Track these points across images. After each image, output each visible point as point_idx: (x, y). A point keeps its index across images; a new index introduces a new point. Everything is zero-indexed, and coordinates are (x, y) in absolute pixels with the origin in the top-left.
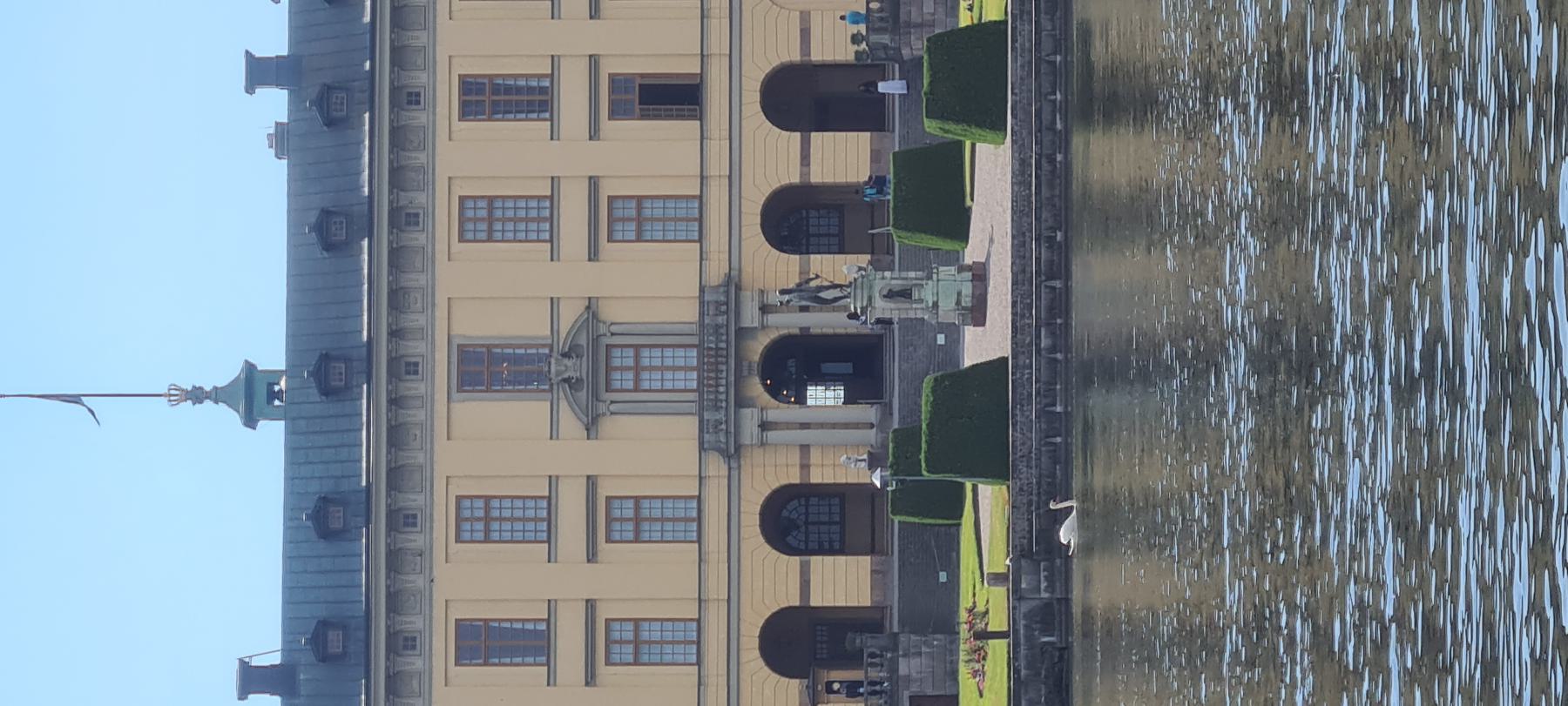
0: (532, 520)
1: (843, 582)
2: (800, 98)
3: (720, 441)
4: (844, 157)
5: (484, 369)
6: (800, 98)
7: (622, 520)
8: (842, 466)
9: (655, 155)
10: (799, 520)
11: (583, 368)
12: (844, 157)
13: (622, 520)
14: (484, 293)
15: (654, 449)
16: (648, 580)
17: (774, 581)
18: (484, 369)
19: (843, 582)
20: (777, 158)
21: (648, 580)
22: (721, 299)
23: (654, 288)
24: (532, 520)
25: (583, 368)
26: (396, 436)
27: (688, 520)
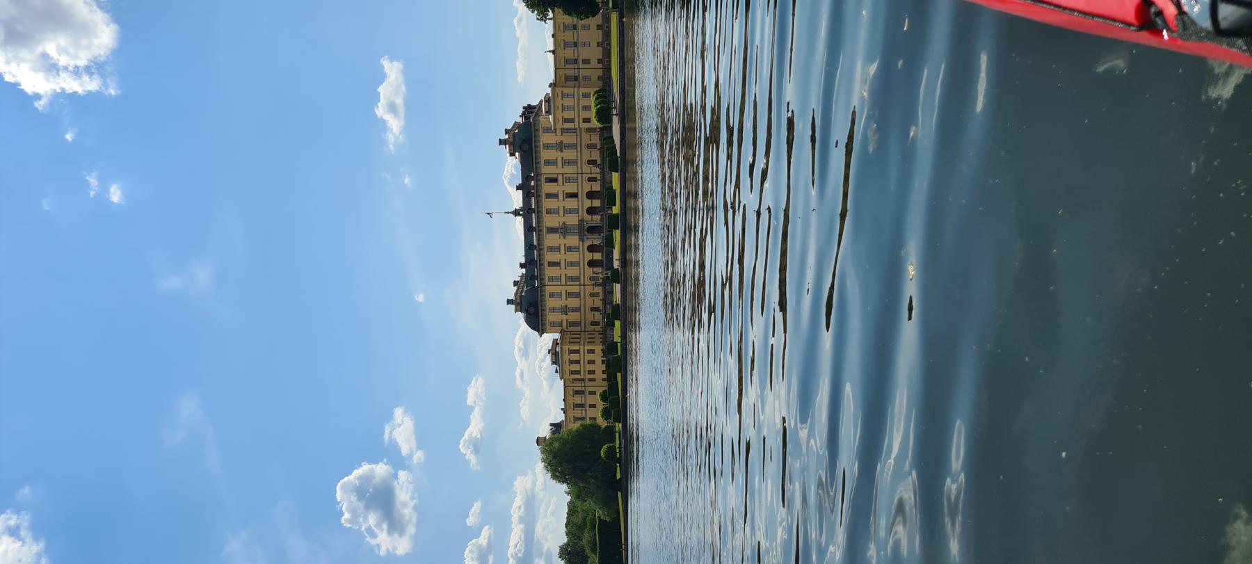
0: (558, 249)
1: (598, 256)
2: (591, 195)
3: (582, 240)
4: (597, 203)
5: (551, 230)
6: (591, 195)
7: (569, 249)
8: (596, 242)
9: (571, 203)
10: (592, 249)
11: (564, 230)
12: (597, 203)
13: (569, 249)
14: (550, 221)
15: (573, 240)
16: (573, 257)
17: (589, 256)
18: (551, 230)
19: (598, 256)
20: (588, 203)
21: (573, 257)
22: (582, 221)
23: (573, 220)
24: (558, 249)
25: (564, 230)
26: (539, 240)
27: (577, 249)
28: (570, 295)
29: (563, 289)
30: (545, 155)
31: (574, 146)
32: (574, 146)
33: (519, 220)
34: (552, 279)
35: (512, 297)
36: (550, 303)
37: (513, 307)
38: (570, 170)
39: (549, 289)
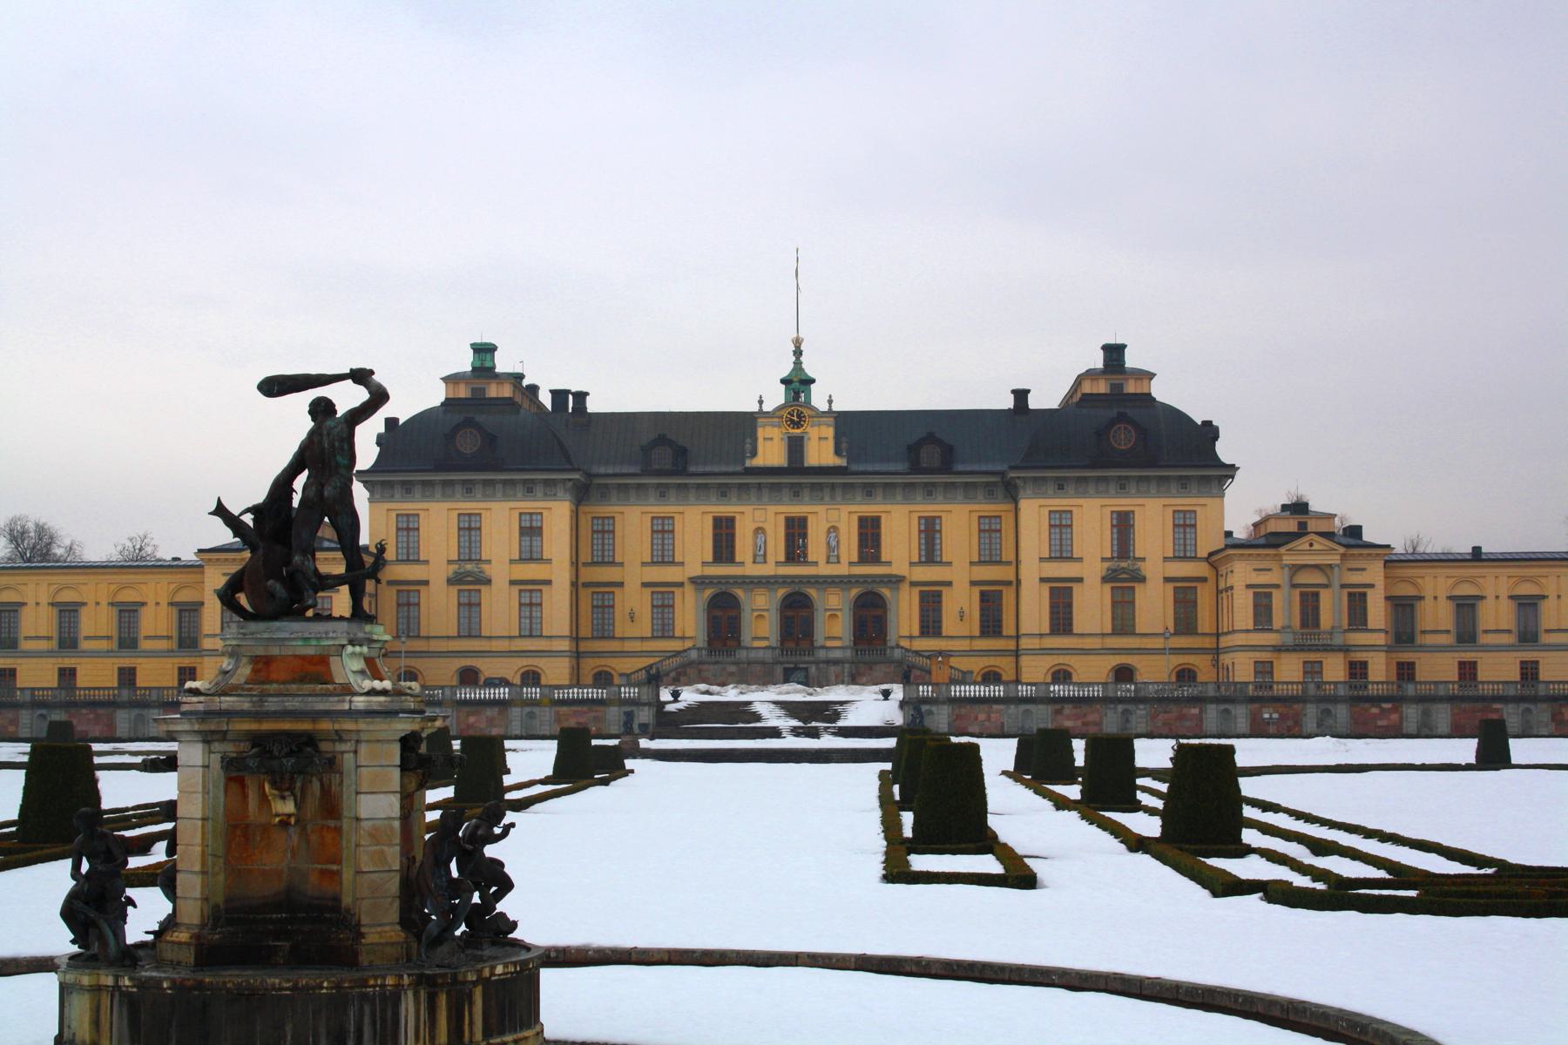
28: (530, 593)
29: (561, 574)
30: (1092, 517)
31: (1123, 622)
32: (1123, 622)
33: (750, 388)
34: (605, 530)
35: (503, 364)
36: (499, 519)
37: (464, 362)
38: (1033, 611)
39: (557, 515)
